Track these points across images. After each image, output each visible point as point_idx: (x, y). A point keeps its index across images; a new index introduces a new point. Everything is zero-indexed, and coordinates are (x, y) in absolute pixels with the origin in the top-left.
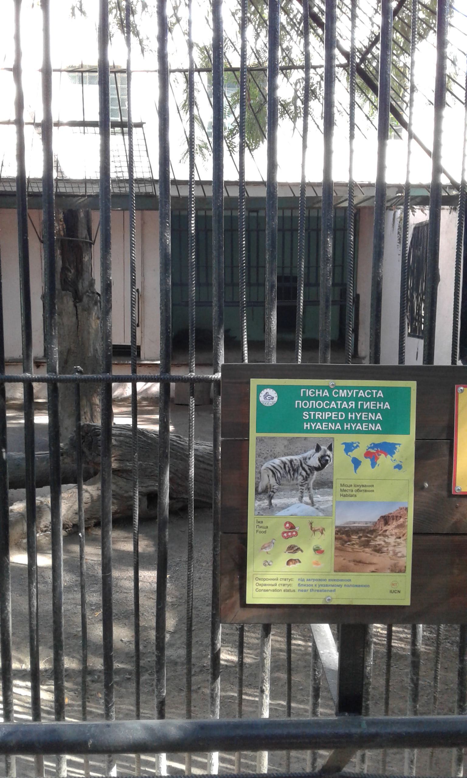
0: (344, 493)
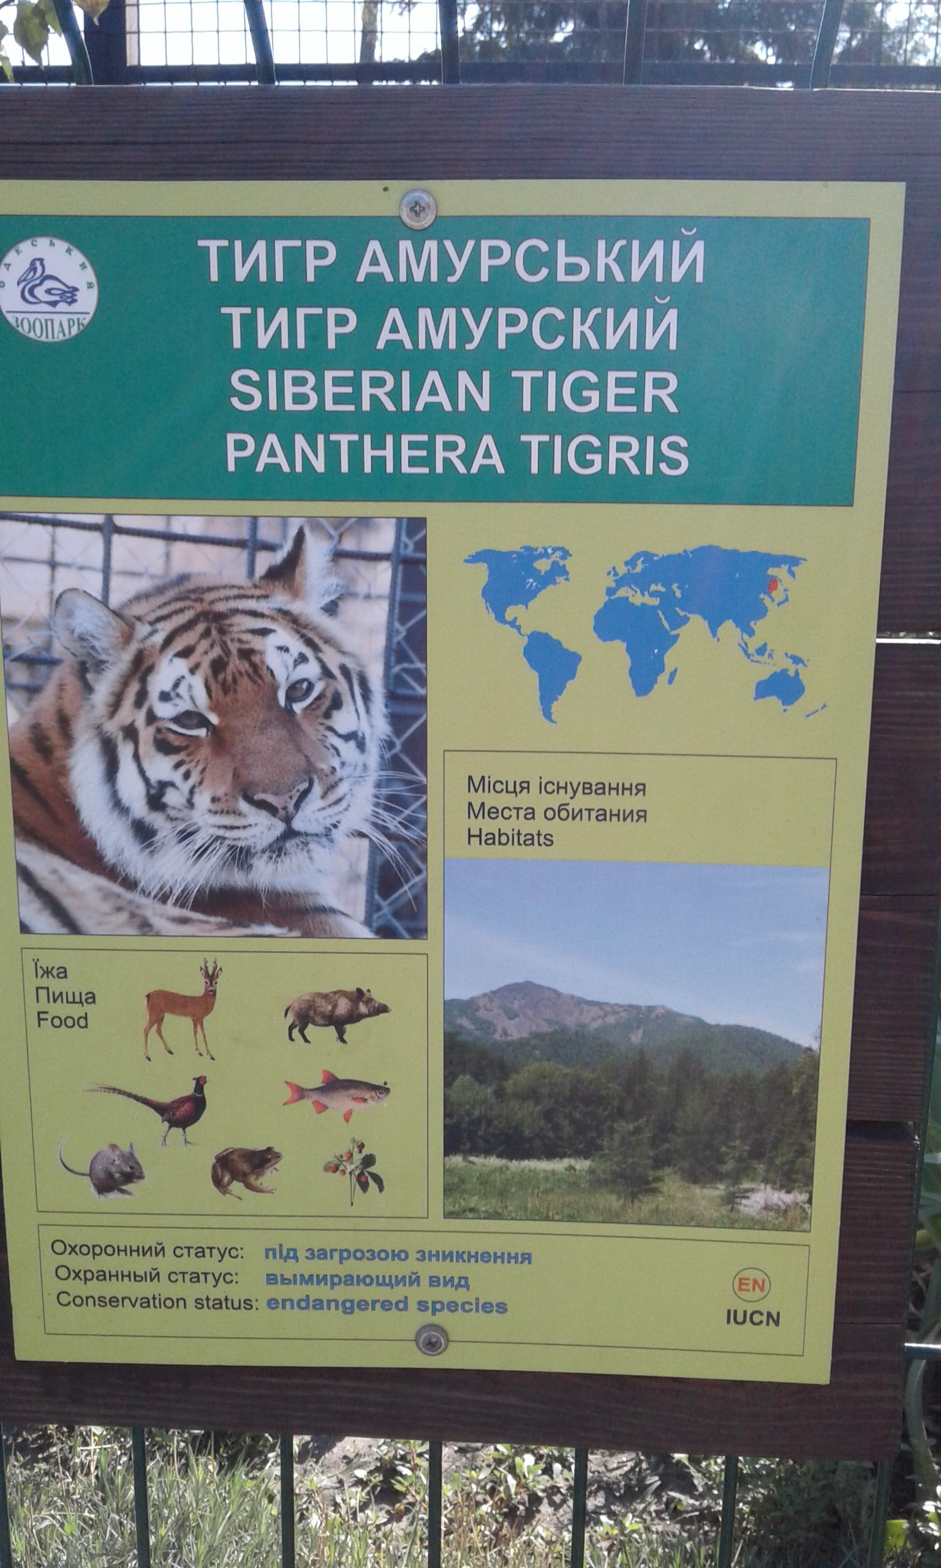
0: (489, 826)
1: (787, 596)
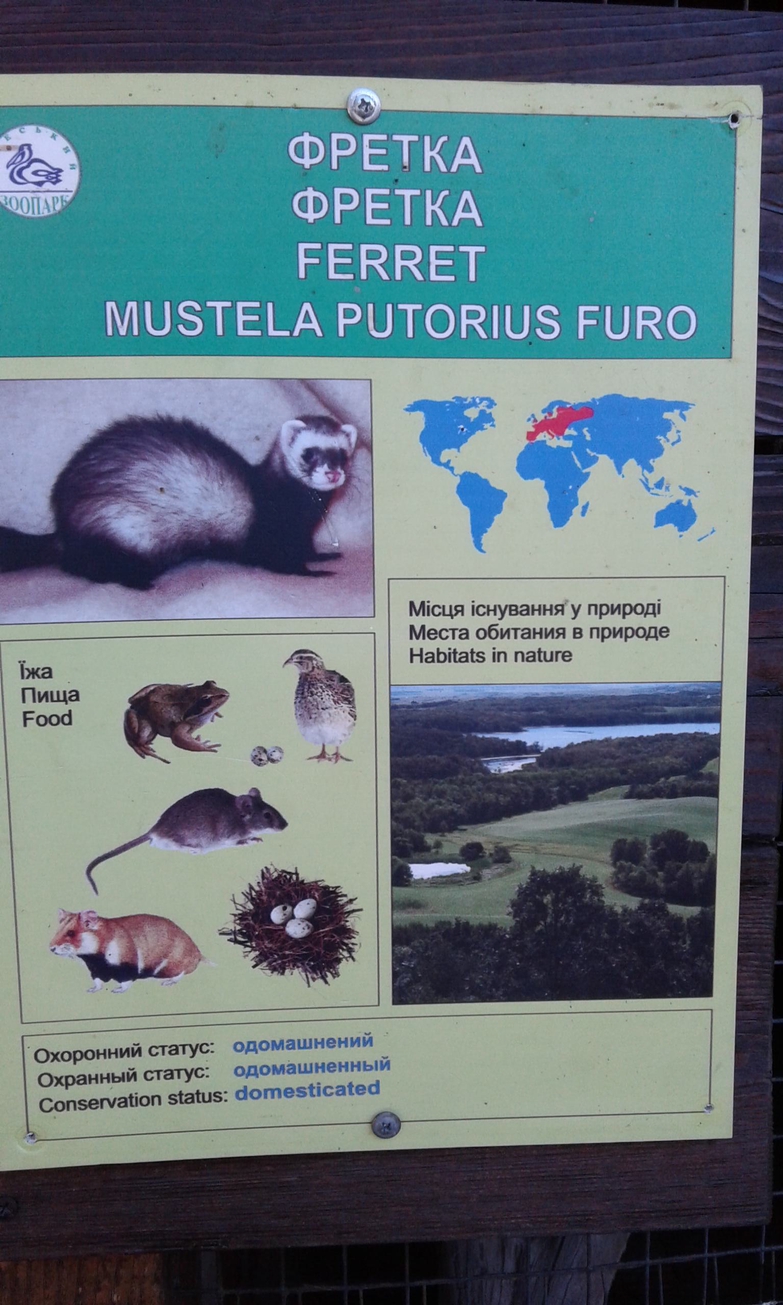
0: (430, 646)
1: (679, 437)
